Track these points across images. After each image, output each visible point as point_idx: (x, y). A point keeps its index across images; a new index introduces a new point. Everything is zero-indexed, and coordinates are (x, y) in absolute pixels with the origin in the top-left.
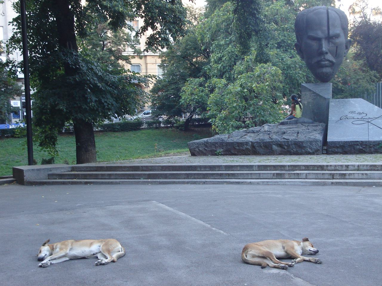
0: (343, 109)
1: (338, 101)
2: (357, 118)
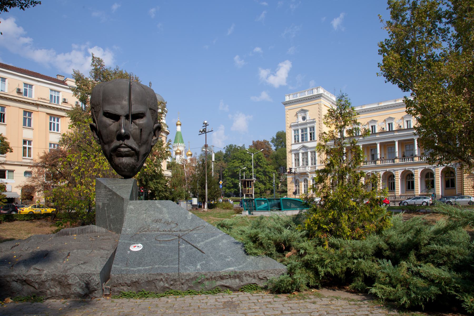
0: (145, 215)
1: (141, 203)
2: (164, 231)
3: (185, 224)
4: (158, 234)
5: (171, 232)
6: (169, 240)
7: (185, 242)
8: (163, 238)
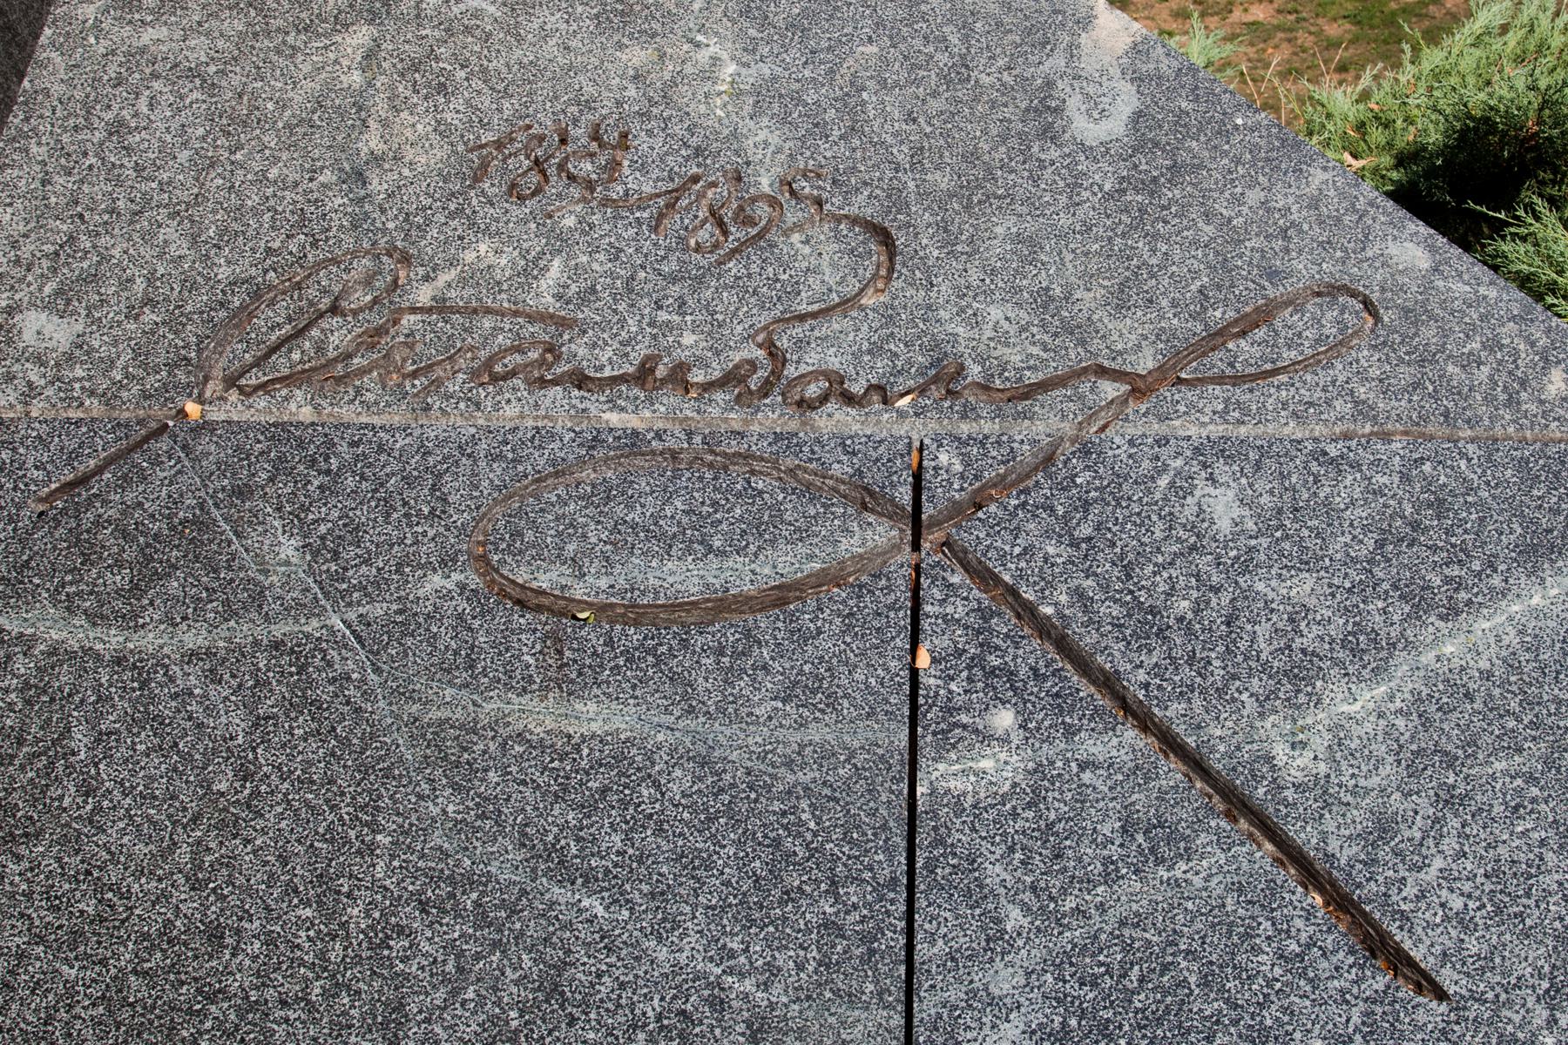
3: (1028, 246)
4: (541, 436)
5: (772, 417)
6: (722, 606)
7: (1033, 652)
8: (622, 540)
